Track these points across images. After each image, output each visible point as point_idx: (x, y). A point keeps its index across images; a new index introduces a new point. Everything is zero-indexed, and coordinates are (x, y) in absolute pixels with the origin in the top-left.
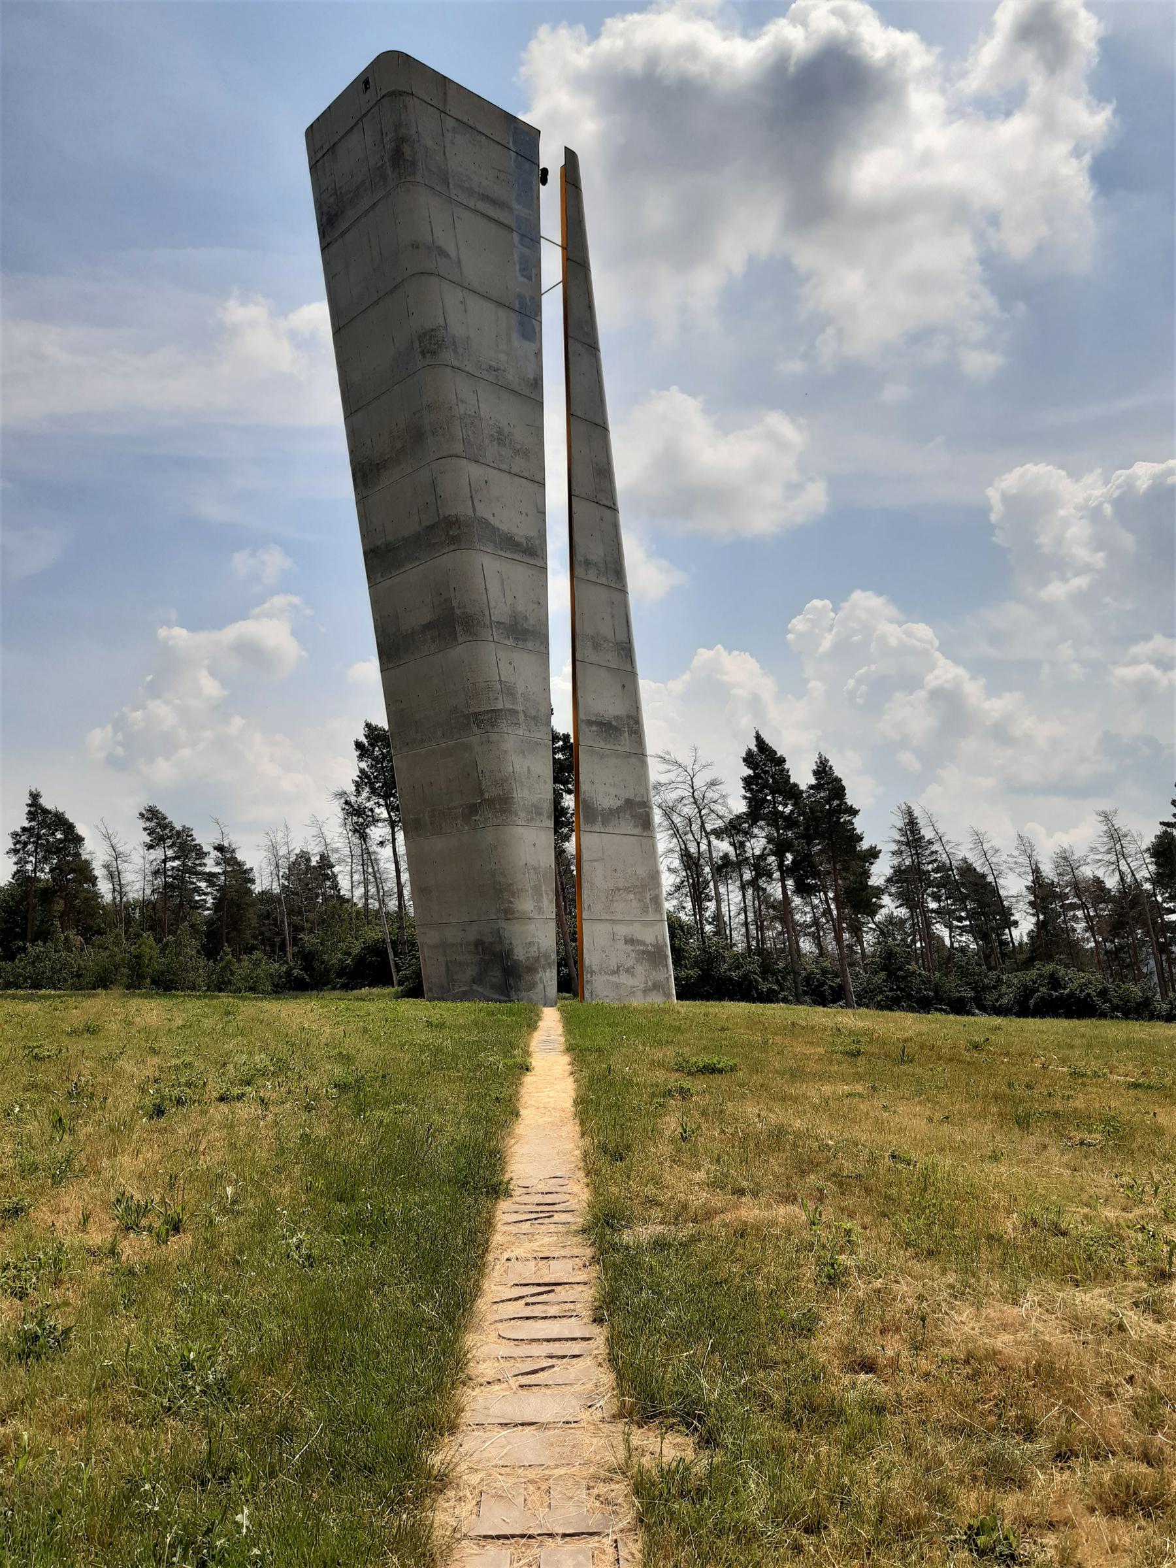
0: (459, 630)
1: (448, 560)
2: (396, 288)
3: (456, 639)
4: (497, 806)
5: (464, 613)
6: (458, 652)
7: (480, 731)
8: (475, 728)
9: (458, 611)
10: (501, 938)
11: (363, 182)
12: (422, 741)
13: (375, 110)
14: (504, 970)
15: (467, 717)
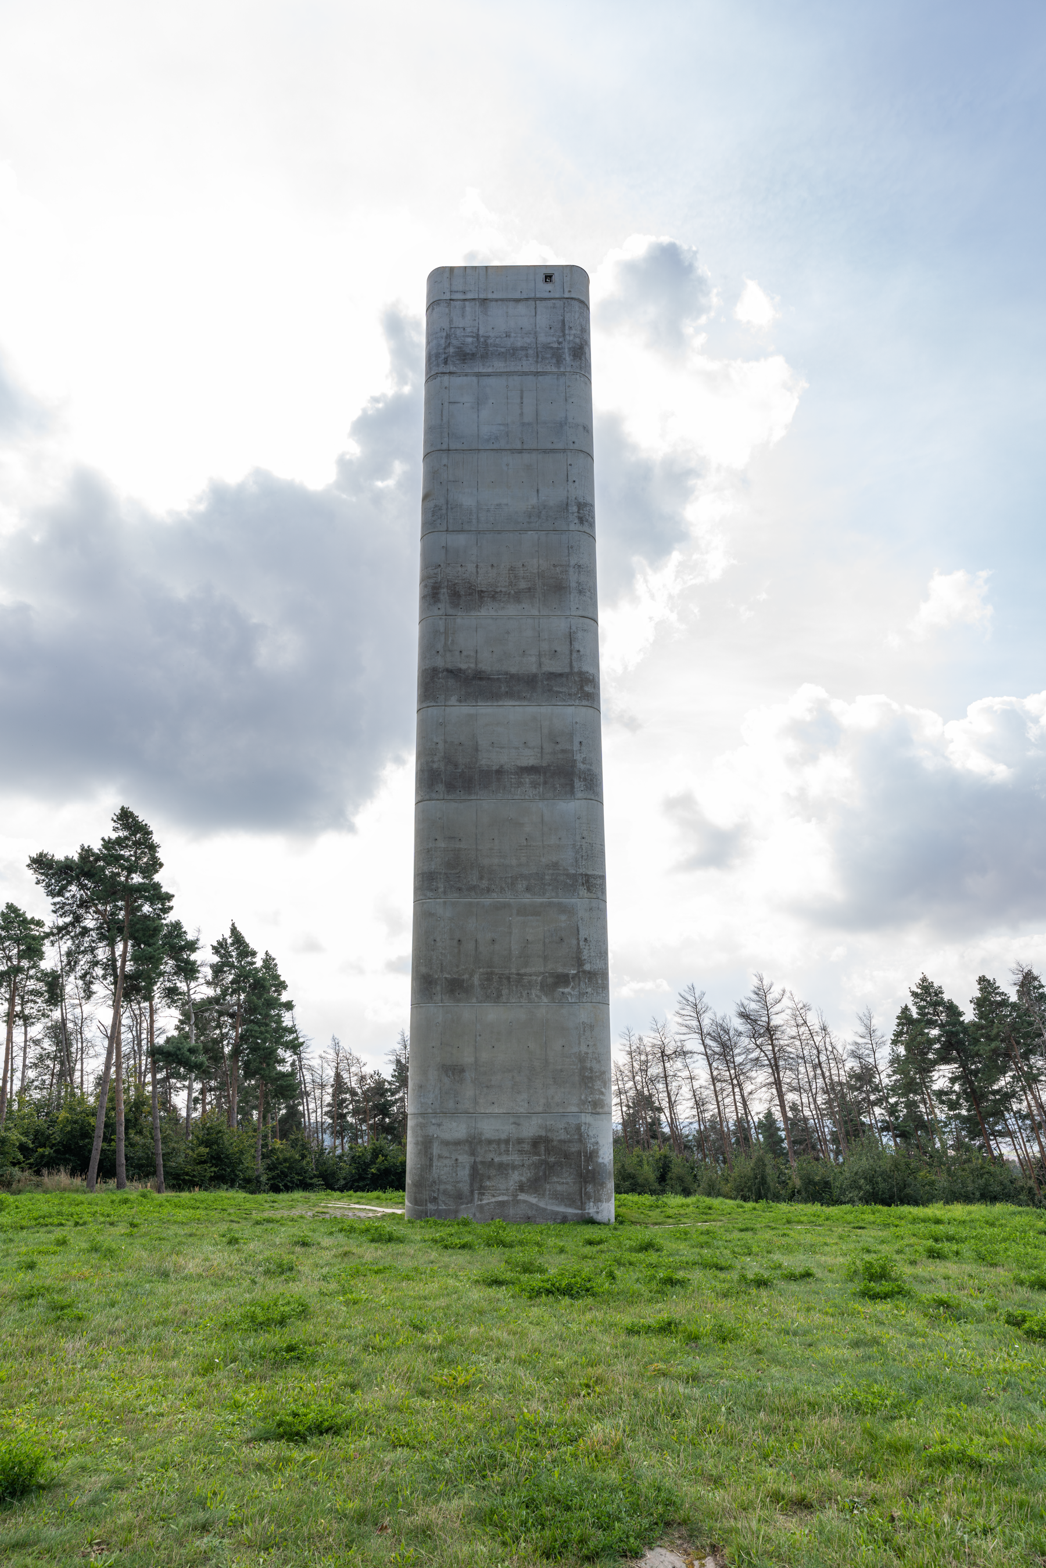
0: (578, 784)
1: (569, 713)
2: (553, 451)
3: (572, 792)
4: (600, 982)
5: (589, 770)
6: (569, 807)
7: (590, 895)
8: (583, 892)
9: (581, 766)
10: (581, 1135)
11: (523, 348)
12: (489, 890)
13: (559, 303)
14: (581, 1175)
15: (574, 877)
